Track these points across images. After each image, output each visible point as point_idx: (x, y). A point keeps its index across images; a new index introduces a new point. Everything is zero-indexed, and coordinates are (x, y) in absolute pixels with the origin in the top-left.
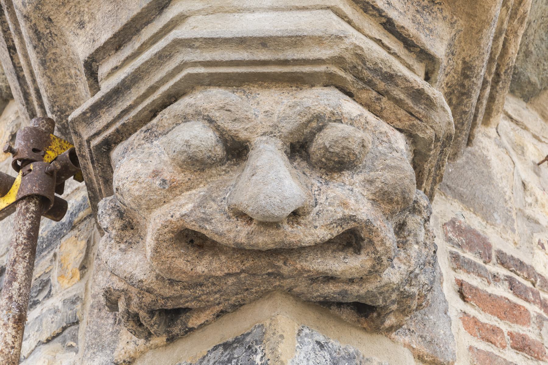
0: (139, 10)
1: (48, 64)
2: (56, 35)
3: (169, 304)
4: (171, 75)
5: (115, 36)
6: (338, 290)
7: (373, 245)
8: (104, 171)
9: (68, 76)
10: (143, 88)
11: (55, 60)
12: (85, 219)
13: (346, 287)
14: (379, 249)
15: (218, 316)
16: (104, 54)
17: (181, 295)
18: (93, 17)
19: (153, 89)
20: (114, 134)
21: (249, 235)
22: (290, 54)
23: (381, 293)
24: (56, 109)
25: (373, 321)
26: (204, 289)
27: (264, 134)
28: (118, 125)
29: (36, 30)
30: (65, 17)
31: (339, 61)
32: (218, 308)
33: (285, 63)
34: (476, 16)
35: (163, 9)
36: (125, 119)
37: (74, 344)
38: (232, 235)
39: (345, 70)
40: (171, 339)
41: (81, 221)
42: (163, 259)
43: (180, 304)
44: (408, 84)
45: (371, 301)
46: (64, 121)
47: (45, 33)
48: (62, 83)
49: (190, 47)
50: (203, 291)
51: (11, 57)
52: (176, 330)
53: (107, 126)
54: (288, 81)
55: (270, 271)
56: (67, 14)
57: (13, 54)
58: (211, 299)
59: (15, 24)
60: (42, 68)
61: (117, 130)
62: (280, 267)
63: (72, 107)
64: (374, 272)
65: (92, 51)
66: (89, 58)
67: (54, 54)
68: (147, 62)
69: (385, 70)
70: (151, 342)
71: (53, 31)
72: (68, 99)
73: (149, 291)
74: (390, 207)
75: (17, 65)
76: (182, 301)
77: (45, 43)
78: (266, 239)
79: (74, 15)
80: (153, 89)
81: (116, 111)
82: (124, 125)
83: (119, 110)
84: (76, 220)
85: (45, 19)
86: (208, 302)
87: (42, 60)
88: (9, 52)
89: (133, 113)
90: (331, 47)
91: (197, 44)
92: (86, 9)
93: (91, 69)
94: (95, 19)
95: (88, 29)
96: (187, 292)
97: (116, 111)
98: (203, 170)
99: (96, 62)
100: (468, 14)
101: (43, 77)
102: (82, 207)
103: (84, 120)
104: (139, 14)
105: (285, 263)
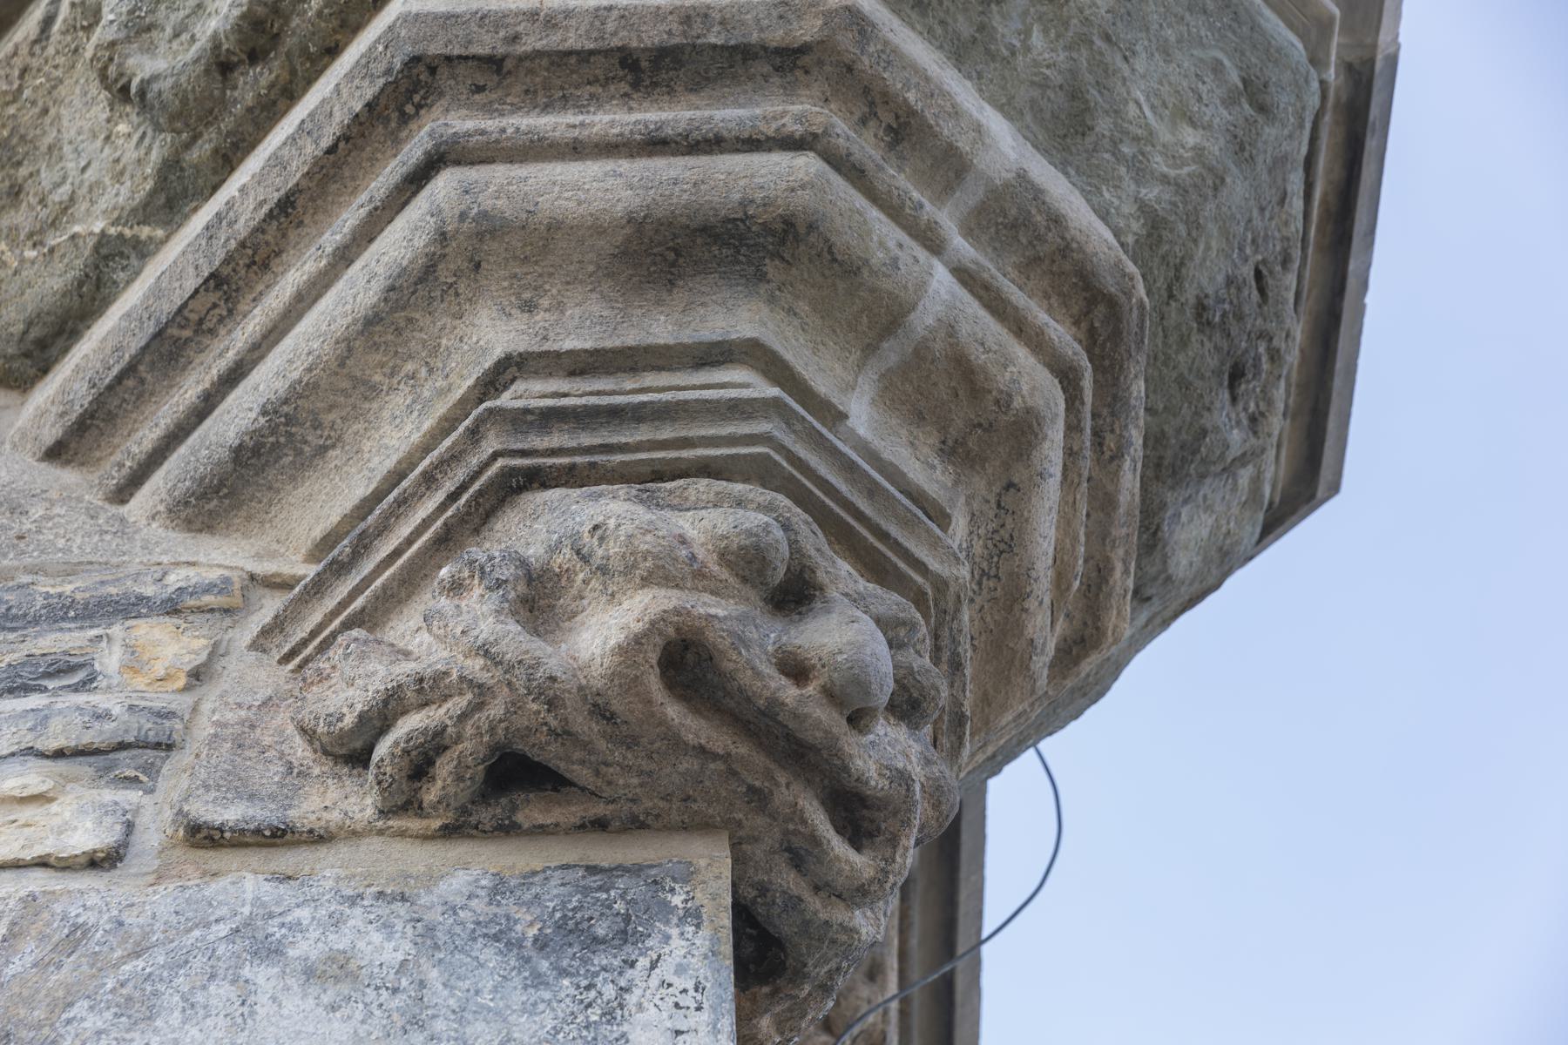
0: (671, 341)
1: (378, 328)
2: (457, 294)
3: (552, 748)
4: (732, 440)
5: (595, 352)
6: (795, 891)
7: (895, 847)
8: (462, 519)
9: (387, 370)
10: (667, 433)
11: (398, 331)
12: (212, 610)
13: (807, 896)
14: (898, 859)
15: (582, 827)
16: (547, 366)
17: (590, 742)
18: (559, 307)
19: (686, 443)
20: (560, 469)
21: (801, 700)
22: (894, 531)
23: (833, 942)
24: (285, 409)
25: (754, 1000)
26: (629, 756)
27: (846, 595)
28: (578, 459)
29: (434, 266)
30: (505, 279)
31: (941, 585)
32: (600, 810)
33: (884, 536)
34: (989, 705)
35: (704, 365)
36: (596, 458)
37: (143, 778)
38: (773, 685)
39: (936, 605)
40: (450, 832)
41: (200, 610)
42: (640, 659)
43: (568, 759)
44: (961, 697)
45: (809, 947)
46: (271, 439)
47: (443, 279)
48: (359, 374)
49: (787, 423)
50: (625, 758)
51: (197, 291)
52: (485, 816)
53: (553, 452)
54: (865, 565)
55: (757, 784)
56: (515, 276)
57: (207, 290)
58: (621, 782)
59: (354, 239)
60: (359, 327)
61: (572, 467)
62: (777, 784)
63: (321, 424)
64: (860, 894)
65: (536, 349)
66: (520, 354)
67: (410, 320)
68: (706, 401)
69: (960, 649)
70: (390, 823)
71: (462, 288)
72: (331, 408)
73: (552, 704)
74: (930, 812)
75: (186, 313)
76: (577, 755)
77: (420, 293)
78: (823, 717)
79: (525, 287)
80: (686, 443)
81: (587, 440)
82: (593, 465)
83: (597, 441)
84: (191, 602)
85: (471, 260)
86: (610, 783)
87: (376, 315)
88: (206, 281)
89: (619, 458)
90: (942, 562)
91: (798, 427)
92: (554, 291)
93: (499, 374)
94: (562, 312)
95: (538, 318)
96: (602, 745)
97: (587, 440)
98: (745, 580)
99: (519, 369)
100: (985, 694)
101: (337, 342)
102: (216, 590)
103: (514, 421)
104: (667, 347)
105: (788, 786)
